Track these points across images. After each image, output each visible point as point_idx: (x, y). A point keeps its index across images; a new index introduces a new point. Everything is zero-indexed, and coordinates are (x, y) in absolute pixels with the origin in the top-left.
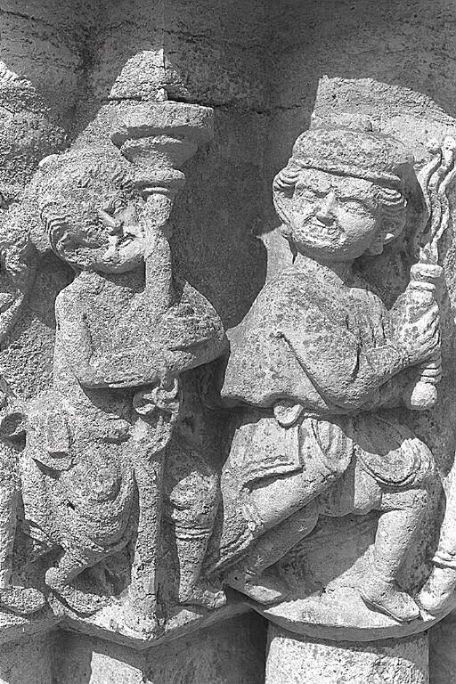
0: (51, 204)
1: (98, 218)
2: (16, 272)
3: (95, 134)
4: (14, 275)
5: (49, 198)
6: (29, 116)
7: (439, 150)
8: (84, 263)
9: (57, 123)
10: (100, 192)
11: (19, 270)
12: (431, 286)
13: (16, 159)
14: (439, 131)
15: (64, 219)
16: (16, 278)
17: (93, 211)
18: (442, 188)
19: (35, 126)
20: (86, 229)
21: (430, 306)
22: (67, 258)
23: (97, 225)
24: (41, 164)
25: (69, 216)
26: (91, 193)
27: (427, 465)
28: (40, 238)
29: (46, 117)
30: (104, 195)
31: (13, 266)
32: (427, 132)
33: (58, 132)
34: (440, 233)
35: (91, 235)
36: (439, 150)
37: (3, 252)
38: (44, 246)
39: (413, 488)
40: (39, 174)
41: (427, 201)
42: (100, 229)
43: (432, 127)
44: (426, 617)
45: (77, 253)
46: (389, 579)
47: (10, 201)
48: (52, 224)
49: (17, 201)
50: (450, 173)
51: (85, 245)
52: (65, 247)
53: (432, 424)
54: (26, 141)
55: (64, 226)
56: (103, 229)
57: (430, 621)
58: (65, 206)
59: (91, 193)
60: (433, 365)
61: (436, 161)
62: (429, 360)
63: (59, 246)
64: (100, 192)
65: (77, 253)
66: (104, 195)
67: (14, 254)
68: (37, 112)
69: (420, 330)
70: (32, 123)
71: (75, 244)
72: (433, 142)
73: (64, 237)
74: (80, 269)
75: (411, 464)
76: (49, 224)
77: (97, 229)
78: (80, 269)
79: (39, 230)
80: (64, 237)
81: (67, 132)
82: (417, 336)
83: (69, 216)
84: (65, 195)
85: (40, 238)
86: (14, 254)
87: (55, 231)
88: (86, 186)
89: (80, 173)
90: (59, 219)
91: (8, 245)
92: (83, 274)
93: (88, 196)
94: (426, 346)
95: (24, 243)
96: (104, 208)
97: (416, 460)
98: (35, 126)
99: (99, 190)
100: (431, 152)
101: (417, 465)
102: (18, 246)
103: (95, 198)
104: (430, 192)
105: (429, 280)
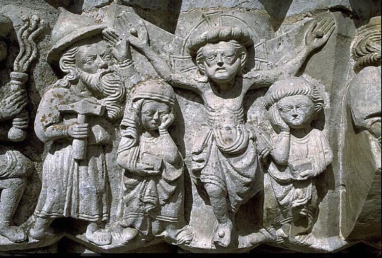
7: (28, 20)
12: (18, 82)
14: (29, 12)
18: (30, 37)
21: (16, 91)
27: (19, 167)
32: (22, 12)
34: (31, 58)
36: (28, 20)
39: (10, 178)
41: (21, 44)
43: (25, 10)
44: (32, 240)
46: (6, 222)
50: (35, 32)
53: (34, 150)
57: (35, 243)
60: (17, 119)
61: (26, 25)
62: (15, 116)
69: (7, 102)
72: (25, 17)
75: (8, 167)
82: (5, 105)
94: (9, 111)
97: (12, 165)
100: (23, 21)
101: (12, 167)
104: (23, 40)
105: (18, 80)
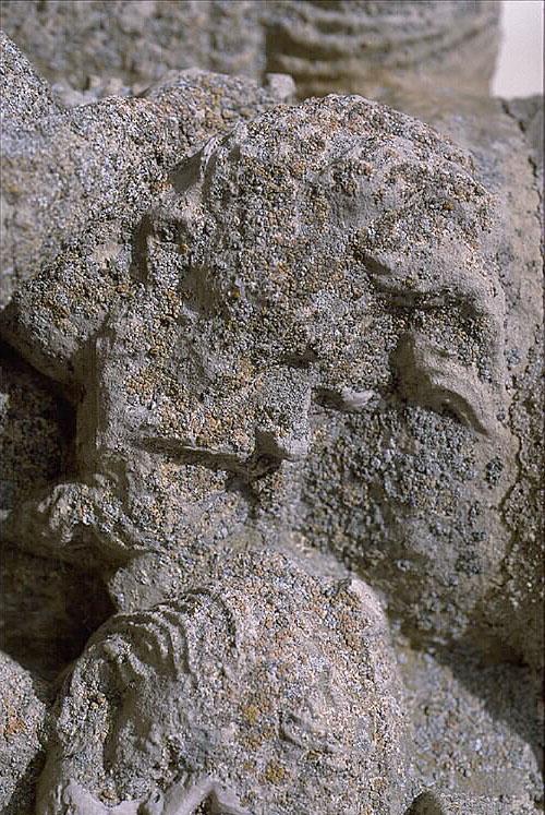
0: (231, 630)
1: (190, 770)
2: (49, 513)
3: (447, 727)
4: (41, 508)
5: (248, 628)
6: (493, 547)
8: (66, 715)
9: (479, 619)
10: (267, 780)
11: (54, 523)
13: (372, 512)
15: (187, 670)
16: (34, 513)
17: (208, 755)
19: (464, 563)
20: (157, 738)
22: (81, 665)
23: (172, 765)
24: (357, 586)
25: (195, 686)
26: (265, 753)
28: (147, 581)
29: (494, 594)
30: (257, 790)
31: (64, 507)
33: (453, 622)
35: (138, 746)
37: (101, 480)
38: (128, 592)
40: (327, 570)
42: (157, 775)
45: (94, 699)
47: (253, 497)
48: (175, 632)
49: (253, 516)
51: (116, 723)
52: (112, 662)
54: (422, 541)
55: (167, 669)
56: (160, 782)
58: (223, 673)
59: (265, 753)
63: (118, 646)
64: (267, 780)
65: (94, 699)
66: (257, 790)
67: (98, 512)
68: (504, 569)
70: (474, 557)
71: (120, 695)
73: (138, 666)
74: (54, 695)
76: (175, 621)
77: (157, 767)
78: (54, 695)
79: (171, 579)
80: (138, 666)
81: (453, 645)
83: (195, 686)
84: (256, 674)
85: (147, 581)
86: (98, 512)
87: (154, 641)
88: (284, 737)
89: (321, 718)
90: (185, 657)
91: (122, 493)
92: (37, 711)
93: (253, 744)
95: (128, 539)
96: (220, 793)
98: (464, 563)
99: (272, 775)
102: (119, 526)
103: (250, 766)
